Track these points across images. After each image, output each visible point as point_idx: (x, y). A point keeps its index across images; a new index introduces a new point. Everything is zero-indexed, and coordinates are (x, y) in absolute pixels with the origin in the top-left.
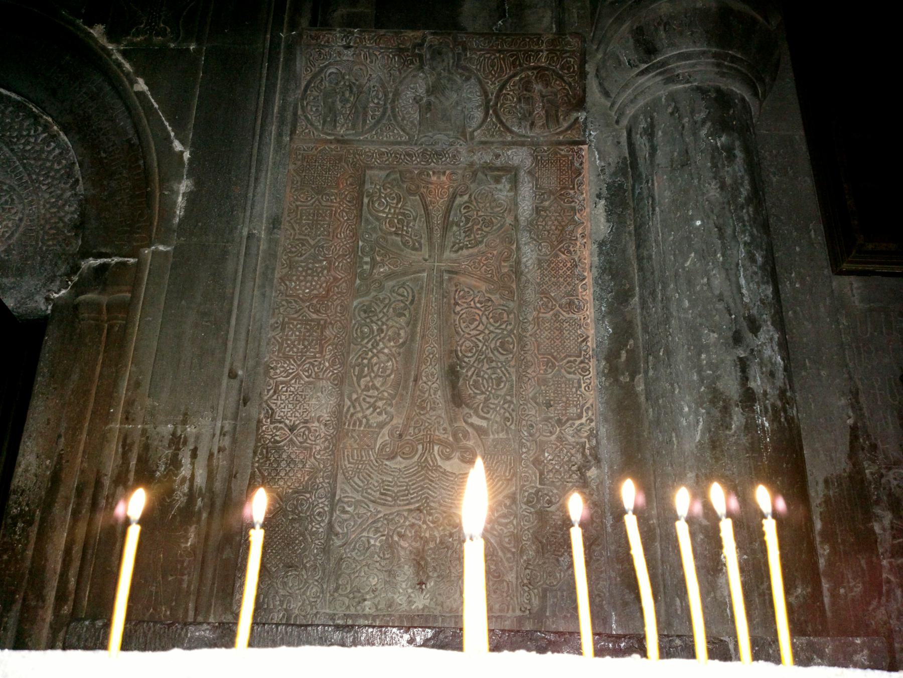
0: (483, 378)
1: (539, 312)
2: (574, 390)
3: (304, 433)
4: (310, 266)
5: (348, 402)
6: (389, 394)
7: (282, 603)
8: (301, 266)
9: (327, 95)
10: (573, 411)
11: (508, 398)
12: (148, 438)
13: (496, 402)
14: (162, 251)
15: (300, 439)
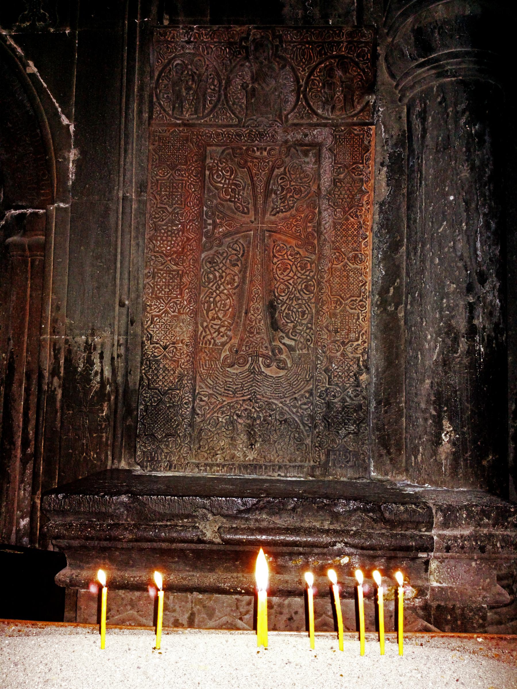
0: (292, 311)
1: (333, 264)
2: (354, 321)
3: (173, 351)
4: (170, 228)
5: (201, 329)
6: (229, 323)
8: (163, 229)
9: (174, 84)
10: (353, 335)
11: (309, 325)
12: (69, 345)
13: (301, 328)
14: (62, 208)
15: (171, 355)
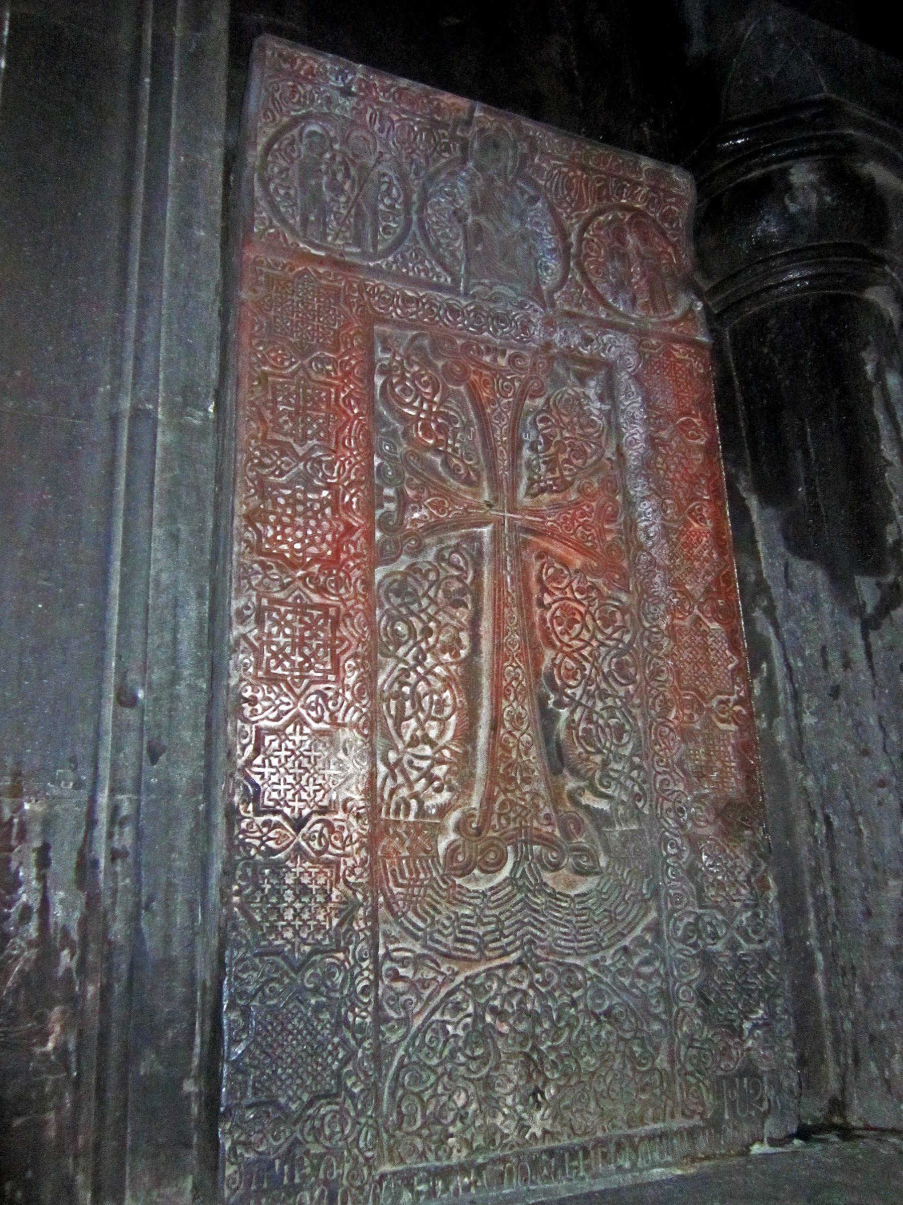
0: (596, 723)
3: (321, 835)
5: (382, 769)
6: (453, 753)
7: (316, 1169)
8: (284, 496)
11: (637, 760)
15: (317, 848)
